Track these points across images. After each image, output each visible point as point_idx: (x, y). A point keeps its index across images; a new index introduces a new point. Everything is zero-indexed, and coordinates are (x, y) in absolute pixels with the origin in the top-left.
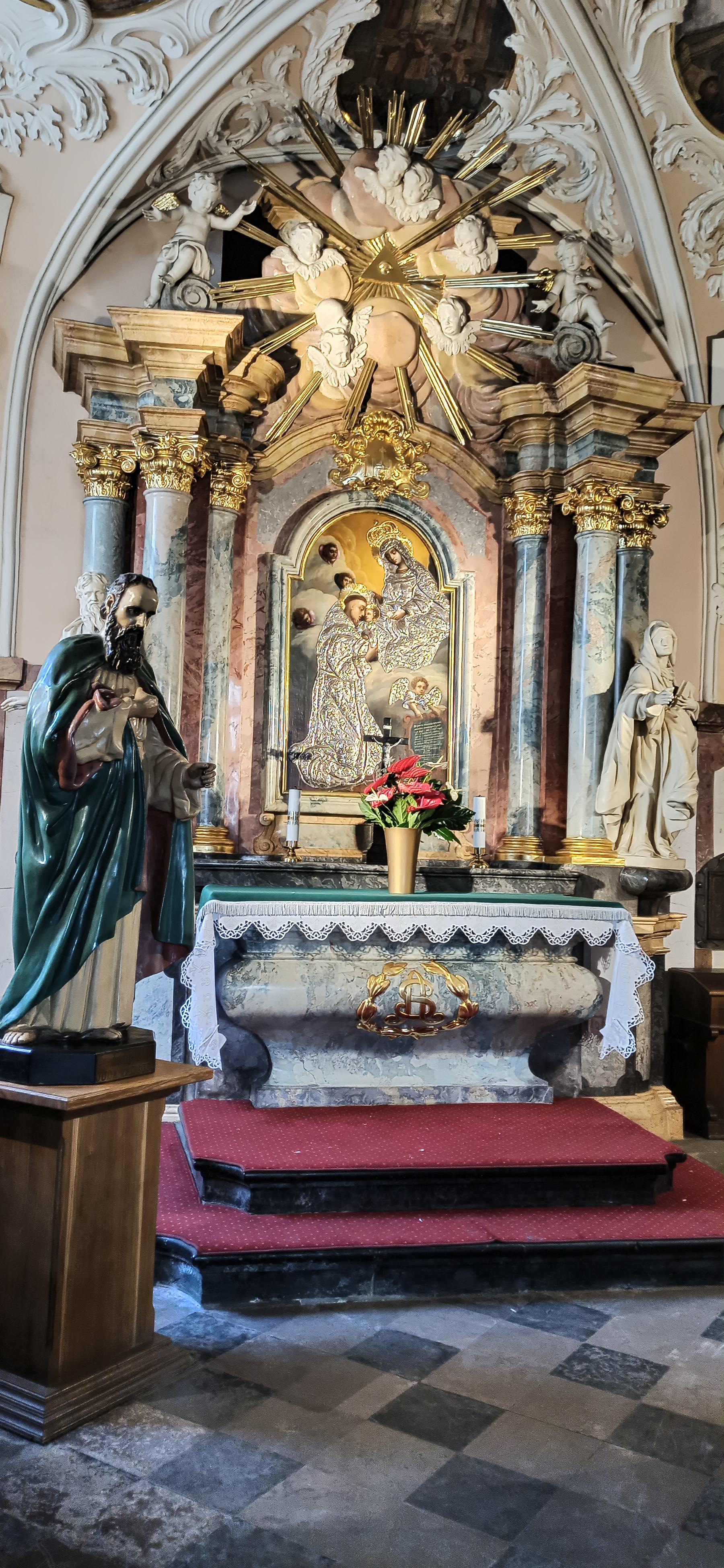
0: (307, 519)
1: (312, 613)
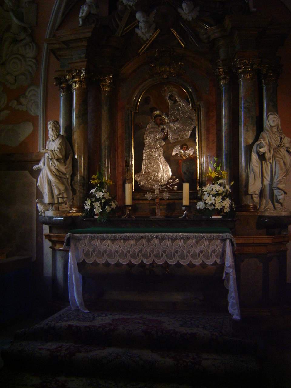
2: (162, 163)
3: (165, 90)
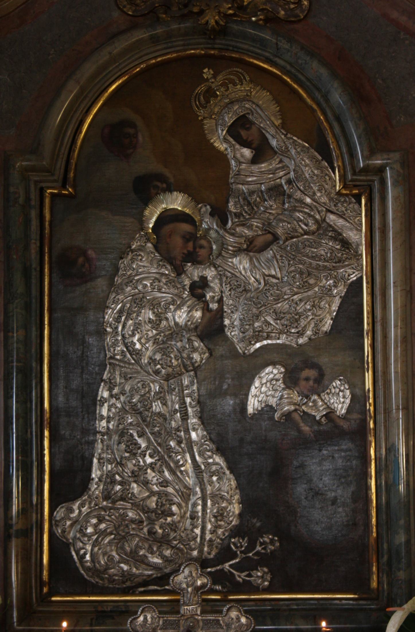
3: (210, 93)
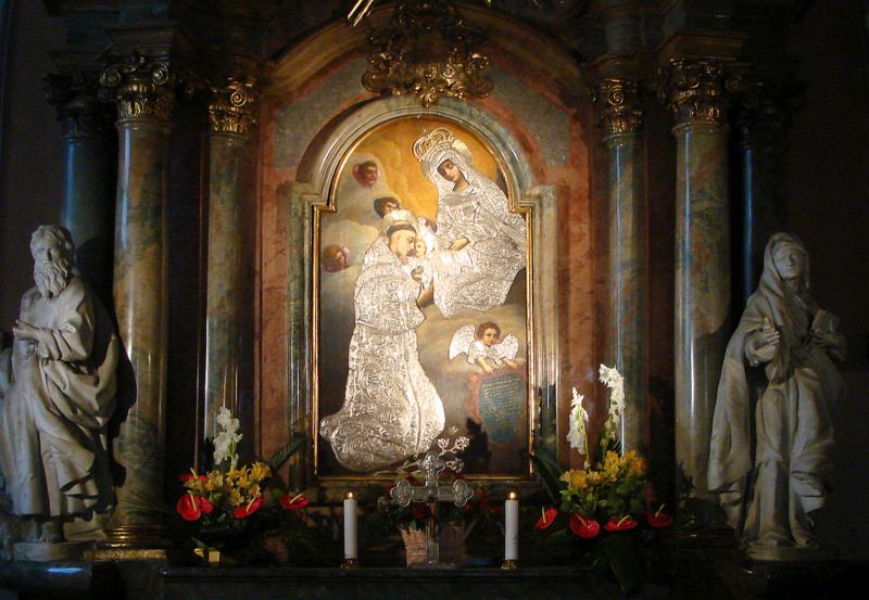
0: (332, 137)
1: (346, 250)
2: (415, 384)
